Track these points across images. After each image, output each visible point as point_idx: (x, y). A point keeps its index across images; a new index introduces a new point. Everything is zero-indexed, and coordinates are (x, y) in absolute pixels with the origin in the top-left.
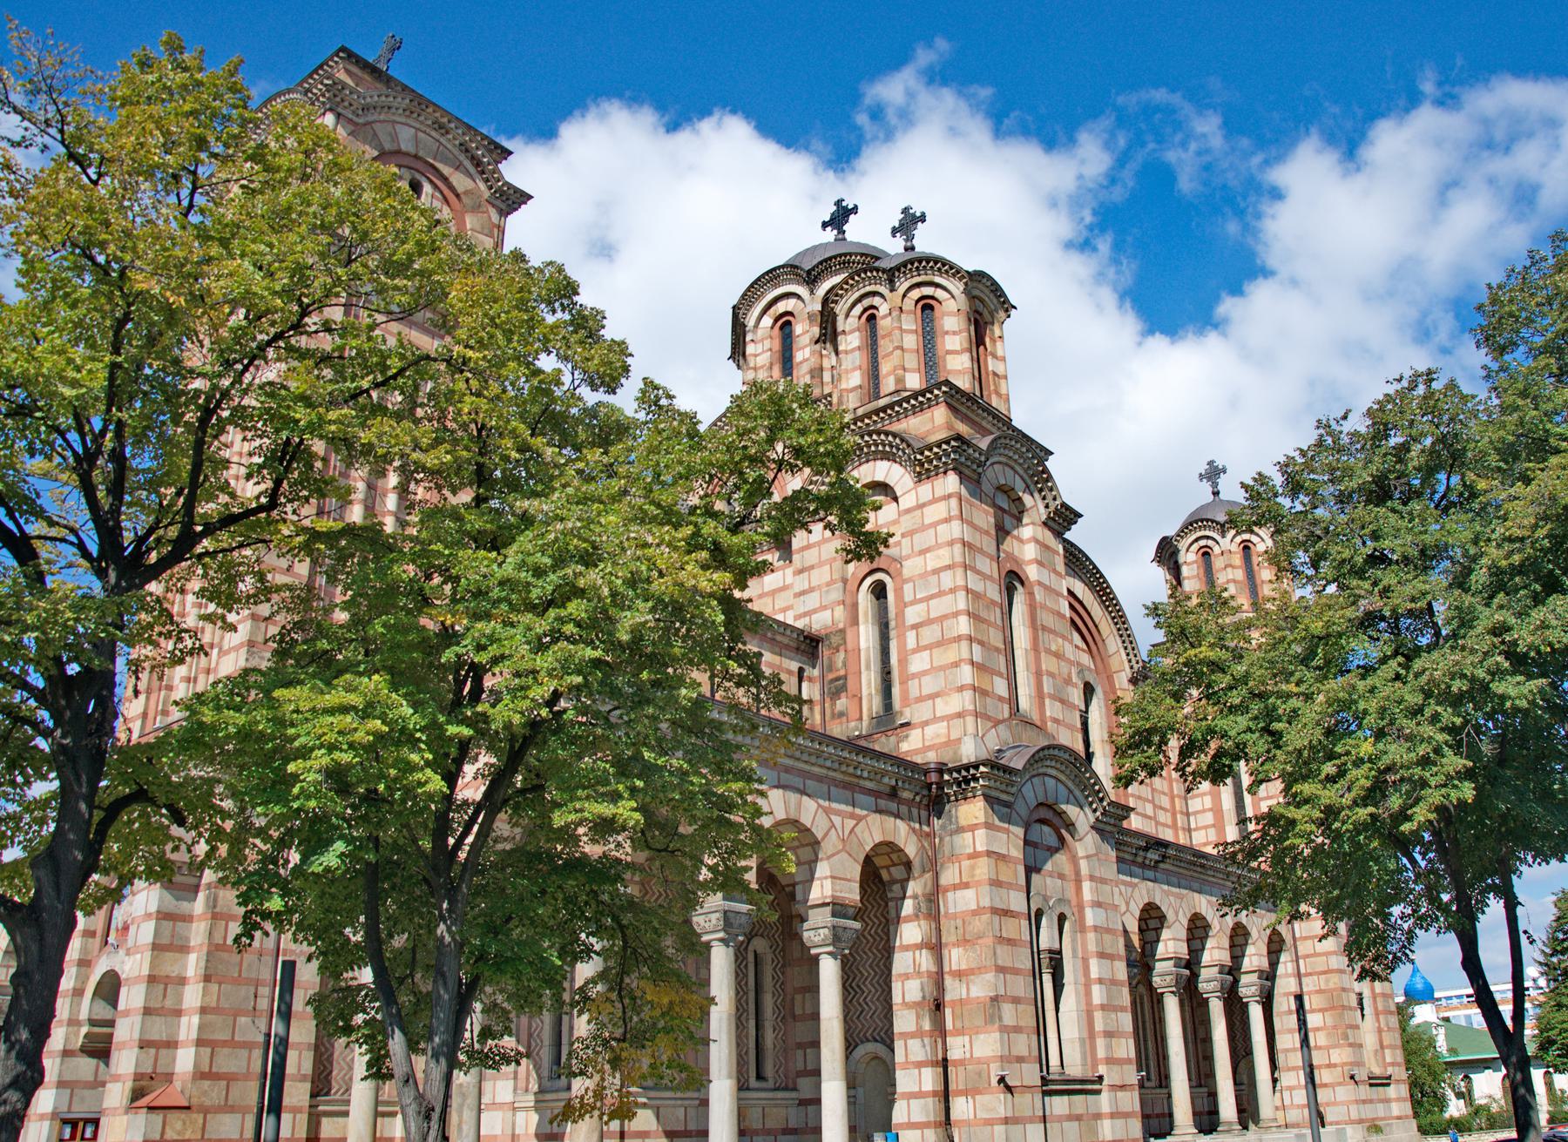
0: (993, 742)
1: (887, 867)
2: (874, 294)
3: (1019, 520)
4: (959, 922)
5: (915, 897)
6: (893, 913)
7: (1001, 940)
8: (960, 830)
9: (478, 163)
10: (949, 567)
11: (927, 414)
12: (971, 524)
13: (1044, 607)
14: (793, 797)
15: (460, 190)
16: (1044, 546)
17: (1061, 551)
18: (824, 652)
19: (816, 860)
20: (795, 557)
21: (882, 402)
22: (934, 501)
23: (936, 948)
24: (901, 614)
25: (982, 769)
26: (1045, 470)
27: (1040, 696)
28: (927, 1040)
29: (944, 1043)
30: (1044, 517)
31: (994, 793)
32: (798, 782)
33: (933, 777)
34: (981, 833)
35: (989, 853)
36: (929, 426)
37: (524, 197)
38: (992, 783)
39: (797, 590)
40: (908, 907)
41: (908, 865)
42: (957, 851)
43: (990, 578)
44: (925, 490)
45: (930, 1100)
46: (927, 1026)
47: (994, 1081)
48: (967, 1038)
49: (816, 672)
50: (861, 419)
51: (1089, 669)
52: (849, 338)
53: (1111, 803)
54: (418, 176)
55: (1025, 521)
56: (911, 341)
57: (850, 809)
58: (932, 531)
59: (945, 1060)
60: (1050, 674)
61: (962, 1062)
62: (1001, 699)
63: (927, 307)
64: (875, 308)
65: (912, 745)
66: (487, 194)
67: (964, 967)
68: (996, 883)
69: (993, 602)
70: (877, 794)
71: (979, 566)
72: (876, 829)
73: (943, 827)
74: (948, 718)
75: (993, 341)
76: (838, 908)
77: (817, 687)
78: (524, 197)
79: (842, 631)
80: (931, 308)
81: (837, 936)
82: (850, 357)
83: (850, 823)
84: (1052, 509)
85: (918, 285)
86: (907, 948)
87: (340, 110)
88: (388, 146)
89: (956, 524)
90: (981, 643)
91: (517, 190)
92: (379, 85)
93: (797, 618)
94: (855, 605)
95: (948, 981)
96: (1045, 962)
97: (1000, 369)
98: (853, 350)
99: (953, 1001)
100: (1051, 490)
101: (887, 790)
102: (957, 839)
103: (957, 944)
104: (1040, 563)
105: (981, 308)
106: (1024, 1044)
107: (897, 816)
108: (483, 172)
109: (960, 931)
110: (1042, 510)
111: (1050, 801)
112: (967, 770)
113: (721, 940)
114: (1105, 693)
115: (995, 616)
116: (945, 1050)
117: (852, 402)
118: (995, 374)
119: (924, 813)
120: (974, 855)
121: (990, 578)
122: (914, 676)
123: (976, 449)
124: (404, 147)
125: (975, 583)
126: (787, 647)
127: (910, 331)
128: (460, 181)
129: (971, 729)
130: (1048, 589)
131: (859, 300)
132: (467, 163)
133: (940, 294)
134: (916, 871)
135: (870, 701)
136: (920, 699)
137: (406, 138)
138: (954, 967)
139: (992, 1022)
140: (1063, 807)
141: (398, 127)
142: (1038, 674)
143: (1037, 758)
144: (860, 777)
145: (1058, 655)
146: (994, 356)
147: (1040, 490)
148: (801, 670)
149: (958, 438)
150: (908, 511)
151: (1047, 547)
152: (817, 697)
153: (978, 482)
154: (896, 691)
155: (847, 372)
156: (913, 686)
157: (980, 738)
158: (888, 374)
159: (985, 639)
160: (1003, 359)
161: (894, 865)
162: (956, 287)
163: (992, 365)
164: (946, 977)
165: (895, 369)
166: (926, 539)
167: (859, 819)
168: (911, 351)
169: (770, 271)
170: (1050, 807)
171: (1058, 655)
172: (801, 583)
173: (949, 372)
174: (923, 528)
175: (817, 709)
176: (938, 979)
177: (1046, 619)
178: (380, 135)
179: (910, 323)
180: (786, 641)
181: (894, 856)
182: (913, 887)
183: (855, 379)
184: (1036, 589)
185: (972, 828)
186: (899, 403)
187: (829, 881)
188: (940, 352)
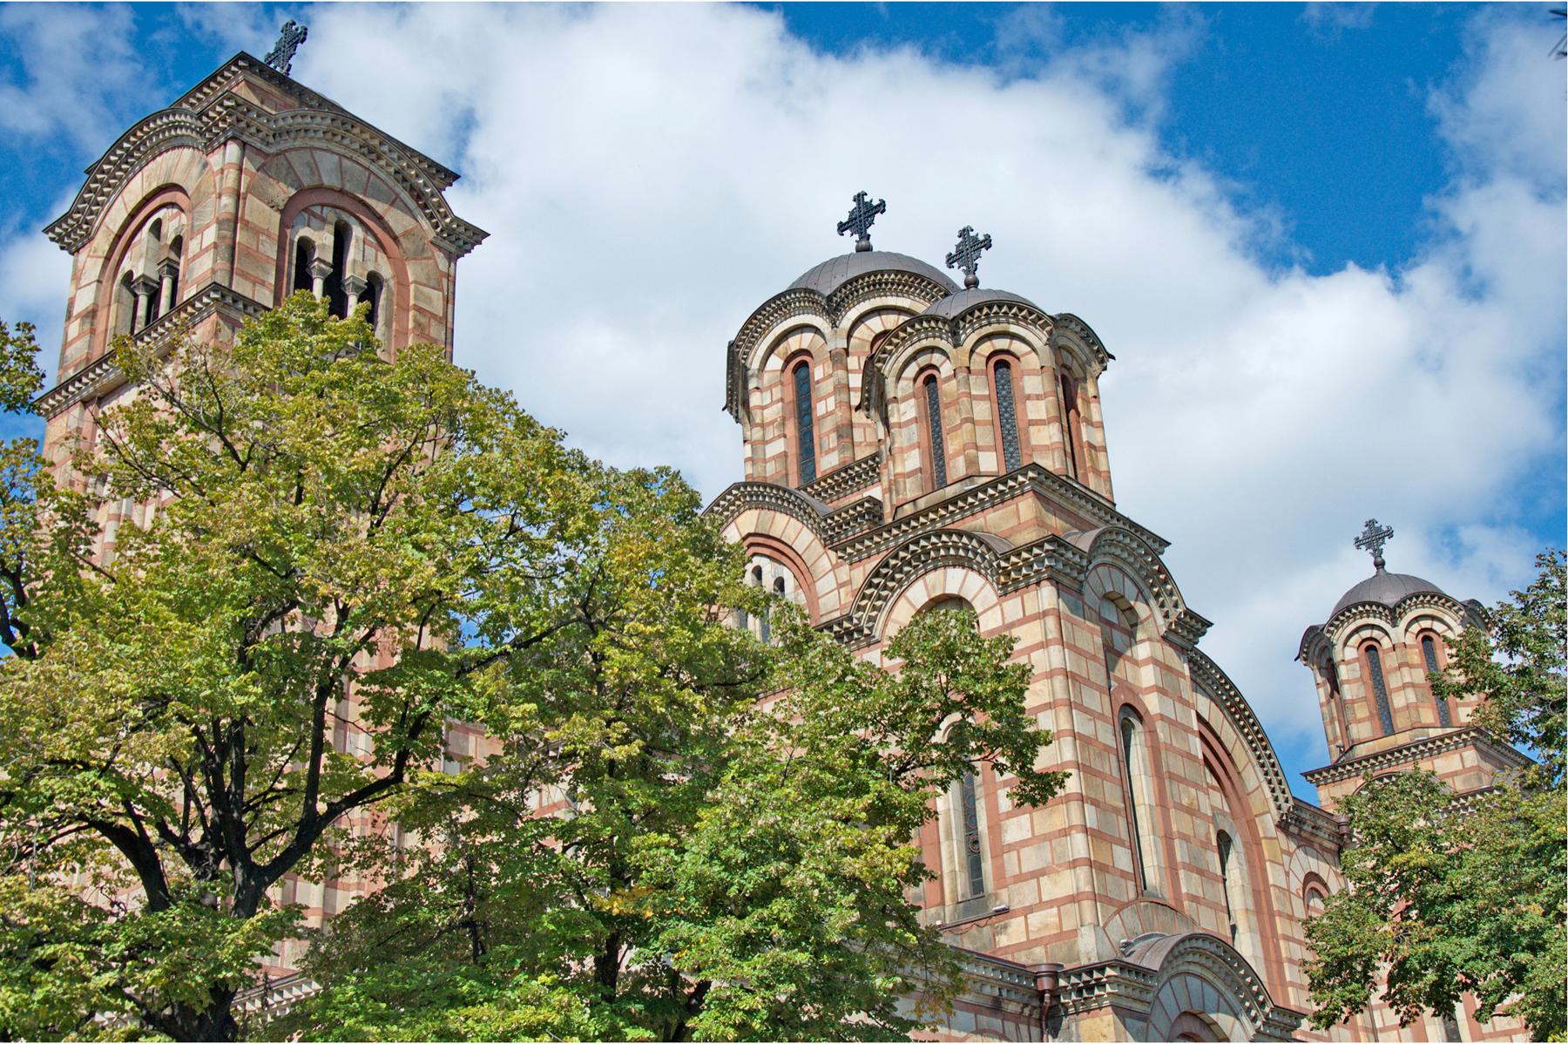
0: (1118, 934)
2: (933, 349)
3: (1132, 635)
9: (418, 195)
11: (1010, 508)
12: (1074, 648)
13: (1170, 748)
15: (398, 231)
16: (1164, 668)
17: (1187, 672)
21: (950, 492)
25: (1109, 972)
26: (1163, 569)
27: (1172, 867)
30: (1163, 630)
31: (1125, 1003)
33: (1045, 984)
36: (1014, 522)
37: (479, 236)
38: (1122, 990)
43: (1101, 716)
44: (1013, 607)
50: (925, 513)
51: (1222, 812)
52: (903, 406)
53: (1276, 1008)
55: (1139, 636)
56: (983, 411)
60: (1184, 837)
62: (1123, 874)
63: (1001, 364)
64: (937, 368)
65: (1011, 938)
66: (431, 234)
69: (1106, 748)
70: (975, 1009)
74: (1058, 903)
75: (1087, 402)
78: (479, 236)
80: (1006, 365)
82: (905, 431)
84: (1173, 618)
85: (989, 337)
88: (307, 181)
90: (1095, 803)
92: (290, 101)
97: (1097, 439)
100: (1171, 594)
101: (989, 1003)
104: (1162, 691)
105: (1068, 360)
108: (425, 207)
110: (1160, 620)
111: (1197, 1009)
112: (1090, 973)
114: (1245, 844)
115: (1110, 766)
117: (911, 489)
118: (1091, 446)
121: (1101, 716)
122: (1012, 847)
123: (1077, 551)
124: (326, 181)
125: (1083, 725)
127: (982, 398)
128: (398, 220)
129: (1089, 917)
130: (1173, 723)
131: (913, 357)
132: (405, 196)
133: (1017, 346)
135: (954, 880)
136: (1021, 878)
140: (1213, 1016)
141: (318, 154)
142: (1168, 838)
143: (1174, 955)
145: (1192, 811)
146: (1089, 423)
147: (1157, 596)
149: (1054, 539)
151: (1169, 669)
153: (1080, 593)
154: (987, 866)
155: (902, 451)
156: (1010, 860)
157: (1101, 928)
158: (957, 454)
159: (1100, 797)
160: (1101, 425)
162: (1038, 337)
163: (1086, 434)
165: (965, 447)
168: (984, 423)
169: (778, 297)
170: (1194, 1015)
171: (1192, 811)
173: (1034, 449)
177: (1175, 764)
178: (299, 168)
179: (980, 386)
183: (913, 461)
184: (1159, 725)
186: (973, 493)
188: (1021, 424)
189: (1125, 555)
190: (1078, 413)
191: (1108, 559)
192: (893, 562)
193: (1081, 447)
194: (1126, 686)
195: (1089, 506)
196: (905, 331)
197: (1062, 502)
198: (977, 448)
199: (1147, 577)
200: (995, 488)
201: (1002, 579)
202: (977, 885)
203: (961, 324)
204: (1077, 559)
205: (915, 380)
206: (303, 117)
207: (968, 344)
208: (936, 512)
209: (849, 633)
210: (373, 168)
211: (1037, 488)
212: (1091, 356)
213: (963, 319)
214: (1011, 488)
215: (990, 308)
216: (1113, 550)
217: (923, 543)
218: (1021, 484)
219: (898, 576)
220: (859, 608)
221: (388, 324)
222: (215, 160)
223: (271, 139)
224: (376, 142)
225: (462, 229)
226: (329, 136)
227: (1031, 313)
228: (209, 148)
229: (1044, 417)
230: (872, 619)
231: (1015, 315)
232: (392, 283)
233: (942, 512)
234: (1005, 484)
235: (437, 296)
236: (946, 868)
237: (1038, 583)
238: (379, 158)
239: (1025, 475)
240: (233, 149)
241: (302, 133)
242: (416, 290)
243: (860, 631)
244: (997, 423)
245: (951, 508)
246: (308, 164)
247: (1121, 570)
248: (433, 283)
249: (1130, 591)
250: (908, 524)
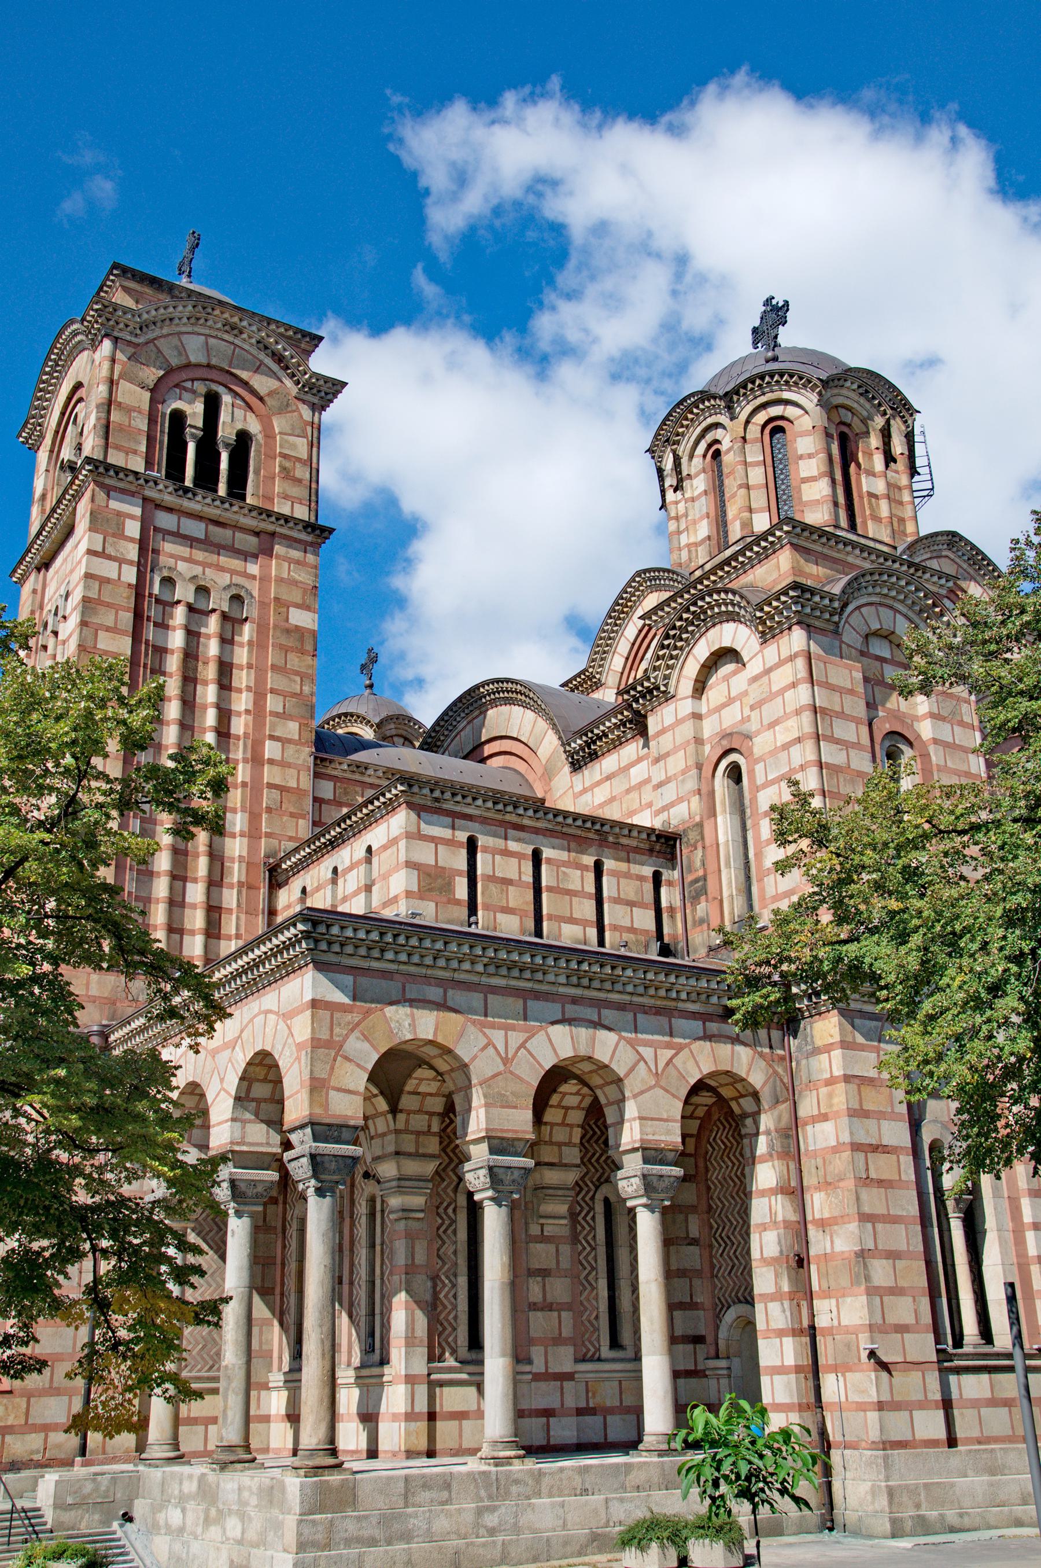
1: (736, 1099)
2: (717, 425)
4: (820, 1161)
5: (768, 1133)
6: (748, 1154)
7: (866, 1181)
8: (816, 1051)
9: (279, 358)
10: (799, 740)
11: (772, 562)
12: (827, 686)
14: (583, 1033)
15: (262, 392)
18: (683, 851)
19: (623, 1100)
20: (652, 744)
21: (728, 553)
22: (781, 663)
23: (795, 1192)
24: (754, 800)
28: (786, 1304)
29: (811, 1307)
32: (591, 1014)
34: (837, 1053)
35: (847, 1078)
36: (775, 575)
37: (337, 386)
39: (655, 782)
40: (762, 1145)
41: (755, 1095)
42: (814, 1077)
43: (857, 746)
44: (771, 652)
45: (793, 1376)
46: (786, 1287)
47: (864, 1355)
48: (833, 1301)
49: (676, 874)
50: (706, 576)
52: (695, 482)
54: (215, 387)
56: (757, 476)
57: (667, 1039)
58: (779, 699)
59: (813, 1327)
61: (829, 1331)
63: (776, 429)
64: (717, 442)
66: (294, 390)
67: (826, 1215)
68: (858, 1113)
70: (704, 1017)
71: (838, 733)
72: (701, 1059)
73: (799, 1048)
76: (651, 1154)
77: (677, 892)
78: (344, 384)
79: (700, 825)
80: (781, 430)
81: (649, 1185)
82: (697, 504)
83: (666, 1054)
86: (763, 1193)
87: (116, 334)
88: (175, 362)
89: (804, 690)
91: (327, 380)
92: (161, 297)
93: (658, 813)
94: (712, 793)
95: (812, 1231)
96: (950, 1204)
98: (699, 496)
99: (818, 1256)
102: (814, 1061)
103: (818, 1189)
105: (848, 417)
106: (912, 1308)
107: (736, 1040)
108: (287, 368)
109: (821, 1172)
113: (492, 1199)
116: (812, 1316)
118: (871, 495)
119: (776, 1034)
120: (831, 1082)
121: (857, 746)
124: (193, 359)
125: (831, 754)
126: (637, 850)
127: (756, 464)
128: (262, 383)
132: (269, 361)
133: (790, 411)
134: (765, 1104)
137: (195, 350)
138: (817, 1216)
139: (859, 1284)
141: (185, 338)
144: (678, 999)
146: (871, 473)
148: (657, 878)
150: (755, 679)
152: (678, 903)
153: (836, 633)
154: (755, 889)
161: (742, 1096)
162: (809, 399)
164: (810, 1226)
165: (740, 511)
166: (772, 710)
167: (680, 1048)
168: (757, 487)
172: (658, 774)
174: (772, 696)
175: (679, 916)
176: (800, 1230)
178: (167, 352)
179: (754, 454)
180: (634, 843)
181: (739, 1086)
182: (766, 1121)
183: (704, 529)
184: (932, 749)
185: (828, 1049)
186: (741, 552)
187: (637, 1123)
188: (794, 483)
189: (893, 593)
190: (859, 465)
191: (874, 599)
192: (678, 624)
193: (861, 497)
194: (896, 715)
195: (857, 552)
196: (692, 413)
197: (826, 551)
198: (751, 511)
199: (921, 611)
200: (759, 545)
201: (760, 628)
202: (751, 907)
203: (735, 398)
204: (827, 602)
205: (704, 456)
206: (165, 308)
207: (743, 416)
208: (715, 574)
209: (650, 691)
210: (236, 341)
211: (795, 541)
212: (873, 410)
213: (737, 393)
214: (772, 543)
215: (762, 378)
216: (878, 590)
217: (700, 603)
218: (779, 538)
219: (684, 636)
220: (655, 669)
221: (257, 472)
222: (97, 356)
223: (138, 332)
224: (236, 319)
225: (322, 382)
227: (801, 378)
228: (94, 346)
229: (815, 473)
230: (667, 677)
231: (787, 382)
232: (260, 437)
233: (720, 573)
234: (766, 540)
236: (726, 894)
237: (790, 629)
238: (241, 333)
239: (781, 529)
240: (107, 345)
241: (168, 322)
242: (281, 439)
243: (658, 688)
244: (771, 485)
245: (727, 569)
246: (176, 347)
247: (891, 607)
249: (902, 626)
250: (695, 588)
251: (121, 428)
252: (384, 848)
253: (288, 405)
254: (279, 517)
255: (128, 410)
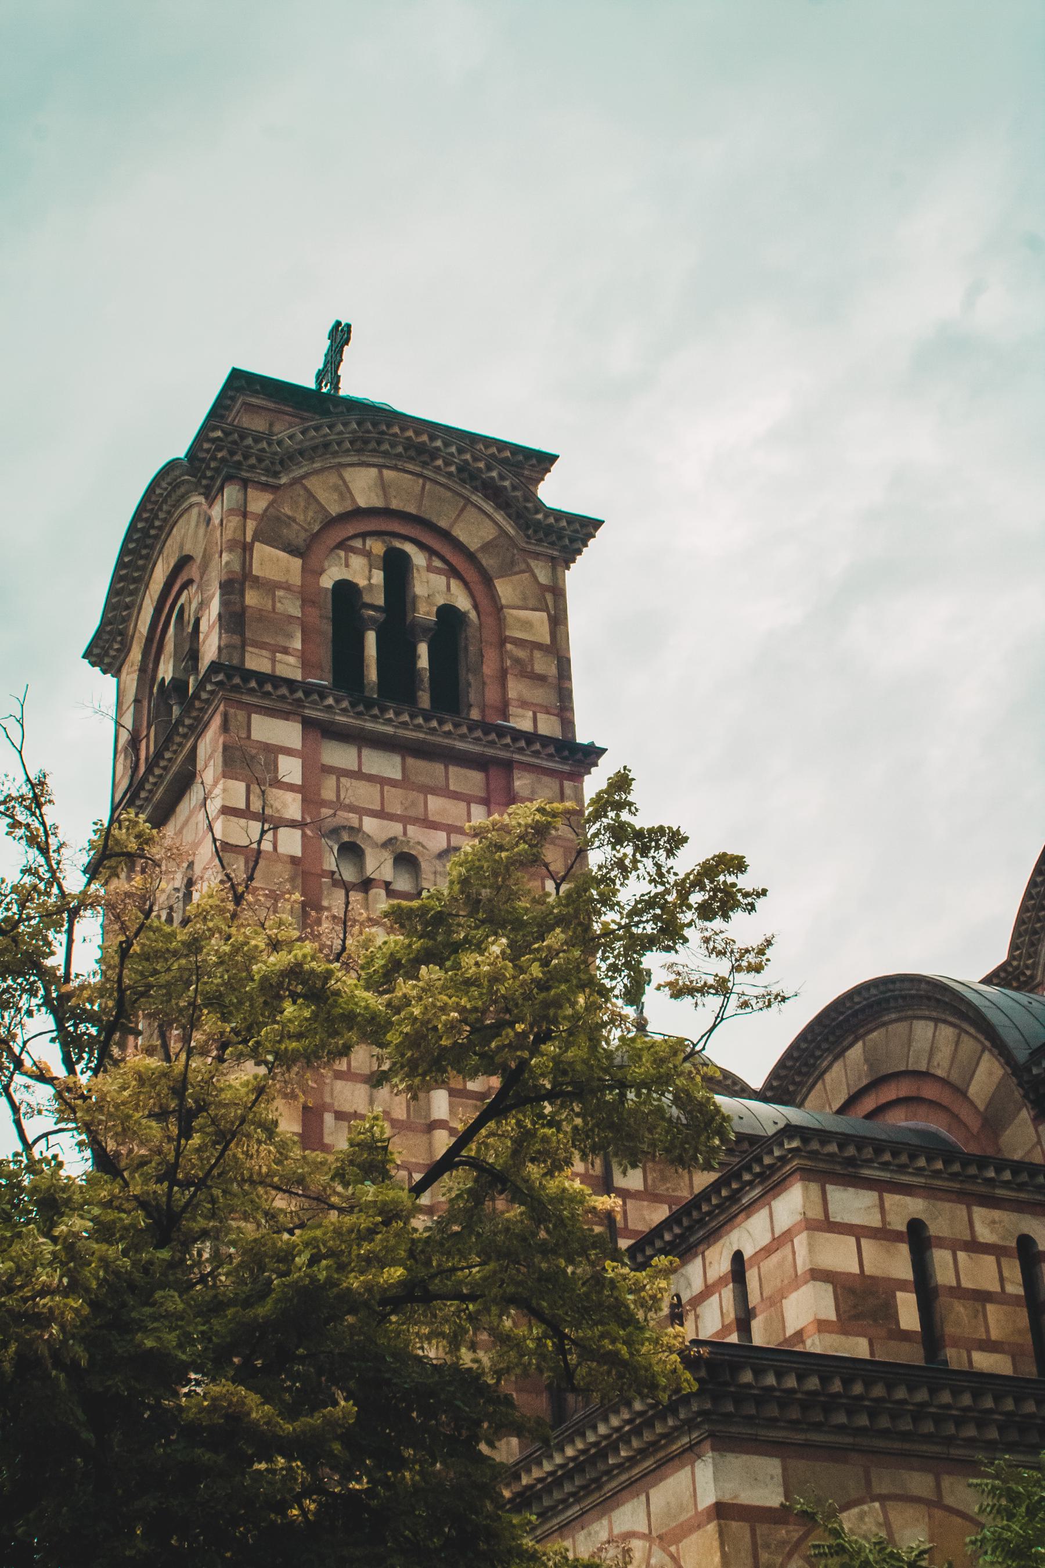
15: (473, 544)
54: (397, 544)
91: (573, 519)
124: (362, 503)
141: (349, 474)
178: (322, 496)
223: (278, 468)
225: (564, 523)
226: (359, 445)
232: (473, 615)
235: (540, 619)
248: (531, 603)
251: (262, 617)
252: (767, 1251)
253: (513, 563)
254: (517, 735)
255: (269, 587)
